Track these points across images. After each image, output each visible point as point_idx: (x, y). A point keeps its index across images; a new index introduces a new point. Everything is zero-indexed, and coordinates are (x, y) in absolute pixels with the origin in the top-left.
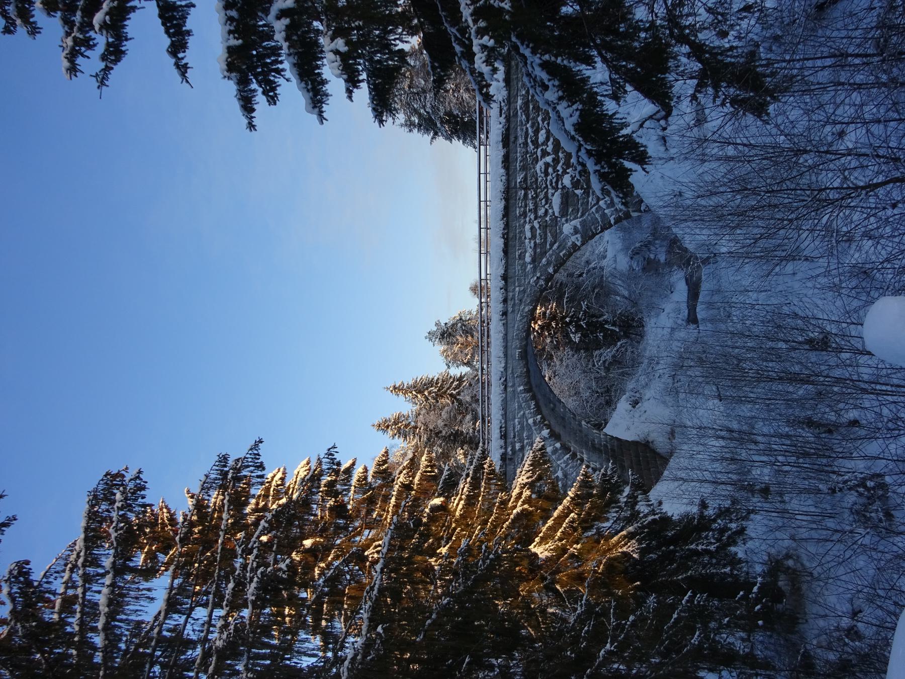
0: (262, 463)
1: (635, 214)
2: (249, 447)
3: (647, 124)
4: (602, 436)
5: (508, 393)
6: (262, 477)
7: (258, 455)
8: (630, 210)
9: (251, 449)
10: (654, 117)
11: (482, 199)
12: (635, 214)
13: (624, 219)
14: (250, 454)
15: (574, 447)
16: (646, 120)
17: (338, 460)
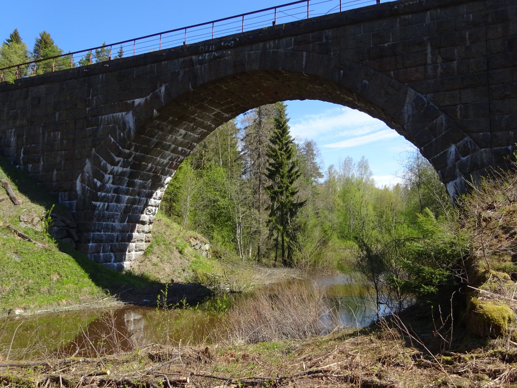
5: (190, 58)
8: (458, 180)
15: (130, 155)
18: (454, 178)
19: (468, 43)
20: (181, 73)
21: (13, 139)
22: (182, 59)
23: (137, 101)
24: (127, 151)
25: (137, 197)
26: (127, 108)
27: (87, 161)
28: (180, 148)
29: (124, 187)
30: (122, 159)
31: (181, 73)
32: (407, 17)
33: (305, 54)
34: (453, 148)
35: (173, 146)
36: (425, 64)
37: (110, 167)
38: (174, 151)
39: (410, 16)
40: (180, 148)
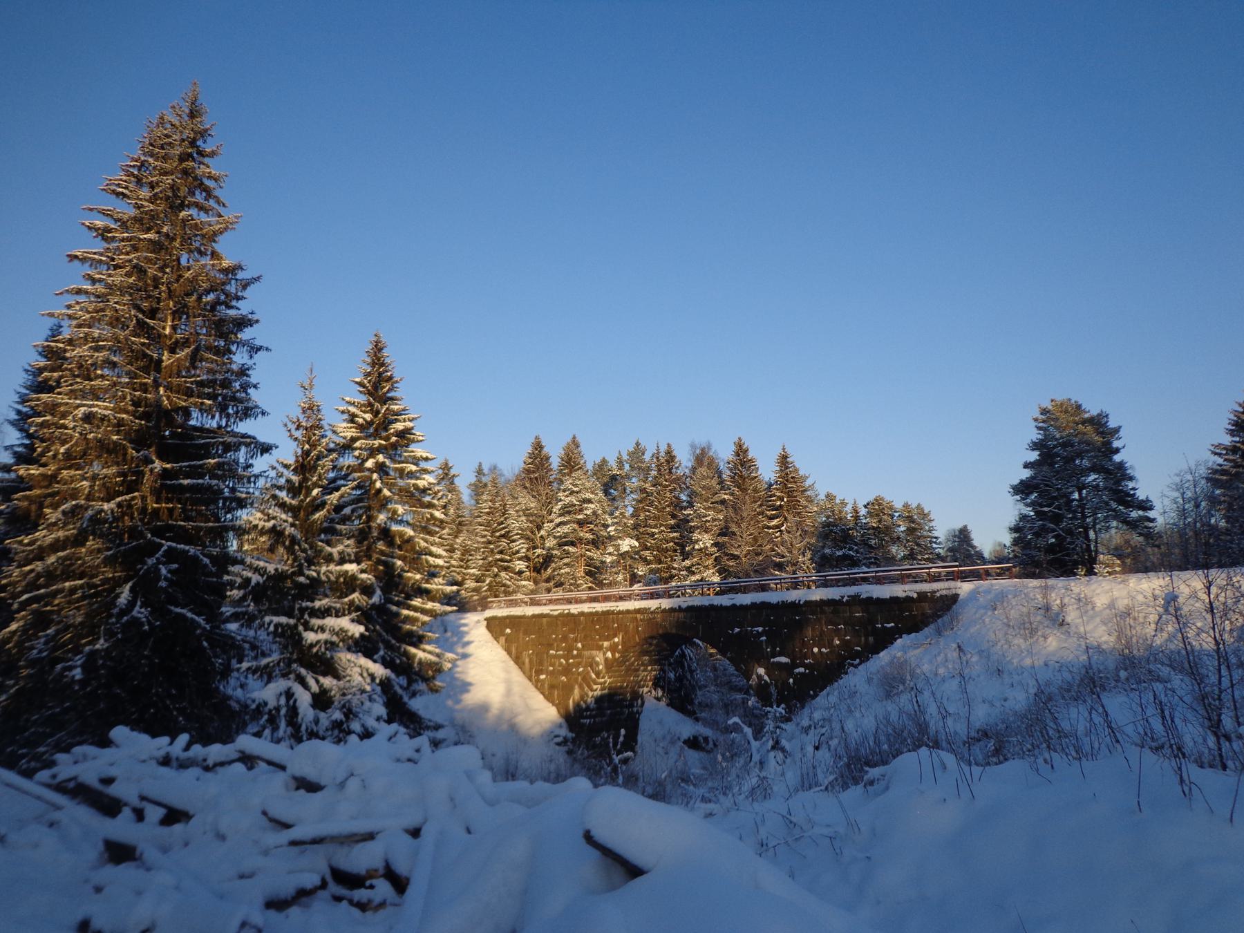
4: (635, 709)
15: (605, 682)
20: (631, 626)
21: (527, 661)
22: (631, 615)
23: (606, 644)
24: (603, 680)
25: (619, 709)
26: (600, 648)
27: (576, 687)
28: (649, 668)
29: (606, 704)
30: (599, 686)
31: (631, 626)
35: (642, 668)
37: (590, 694)
38: (644, 671)
39: (754, 611)
40: (649, 668)
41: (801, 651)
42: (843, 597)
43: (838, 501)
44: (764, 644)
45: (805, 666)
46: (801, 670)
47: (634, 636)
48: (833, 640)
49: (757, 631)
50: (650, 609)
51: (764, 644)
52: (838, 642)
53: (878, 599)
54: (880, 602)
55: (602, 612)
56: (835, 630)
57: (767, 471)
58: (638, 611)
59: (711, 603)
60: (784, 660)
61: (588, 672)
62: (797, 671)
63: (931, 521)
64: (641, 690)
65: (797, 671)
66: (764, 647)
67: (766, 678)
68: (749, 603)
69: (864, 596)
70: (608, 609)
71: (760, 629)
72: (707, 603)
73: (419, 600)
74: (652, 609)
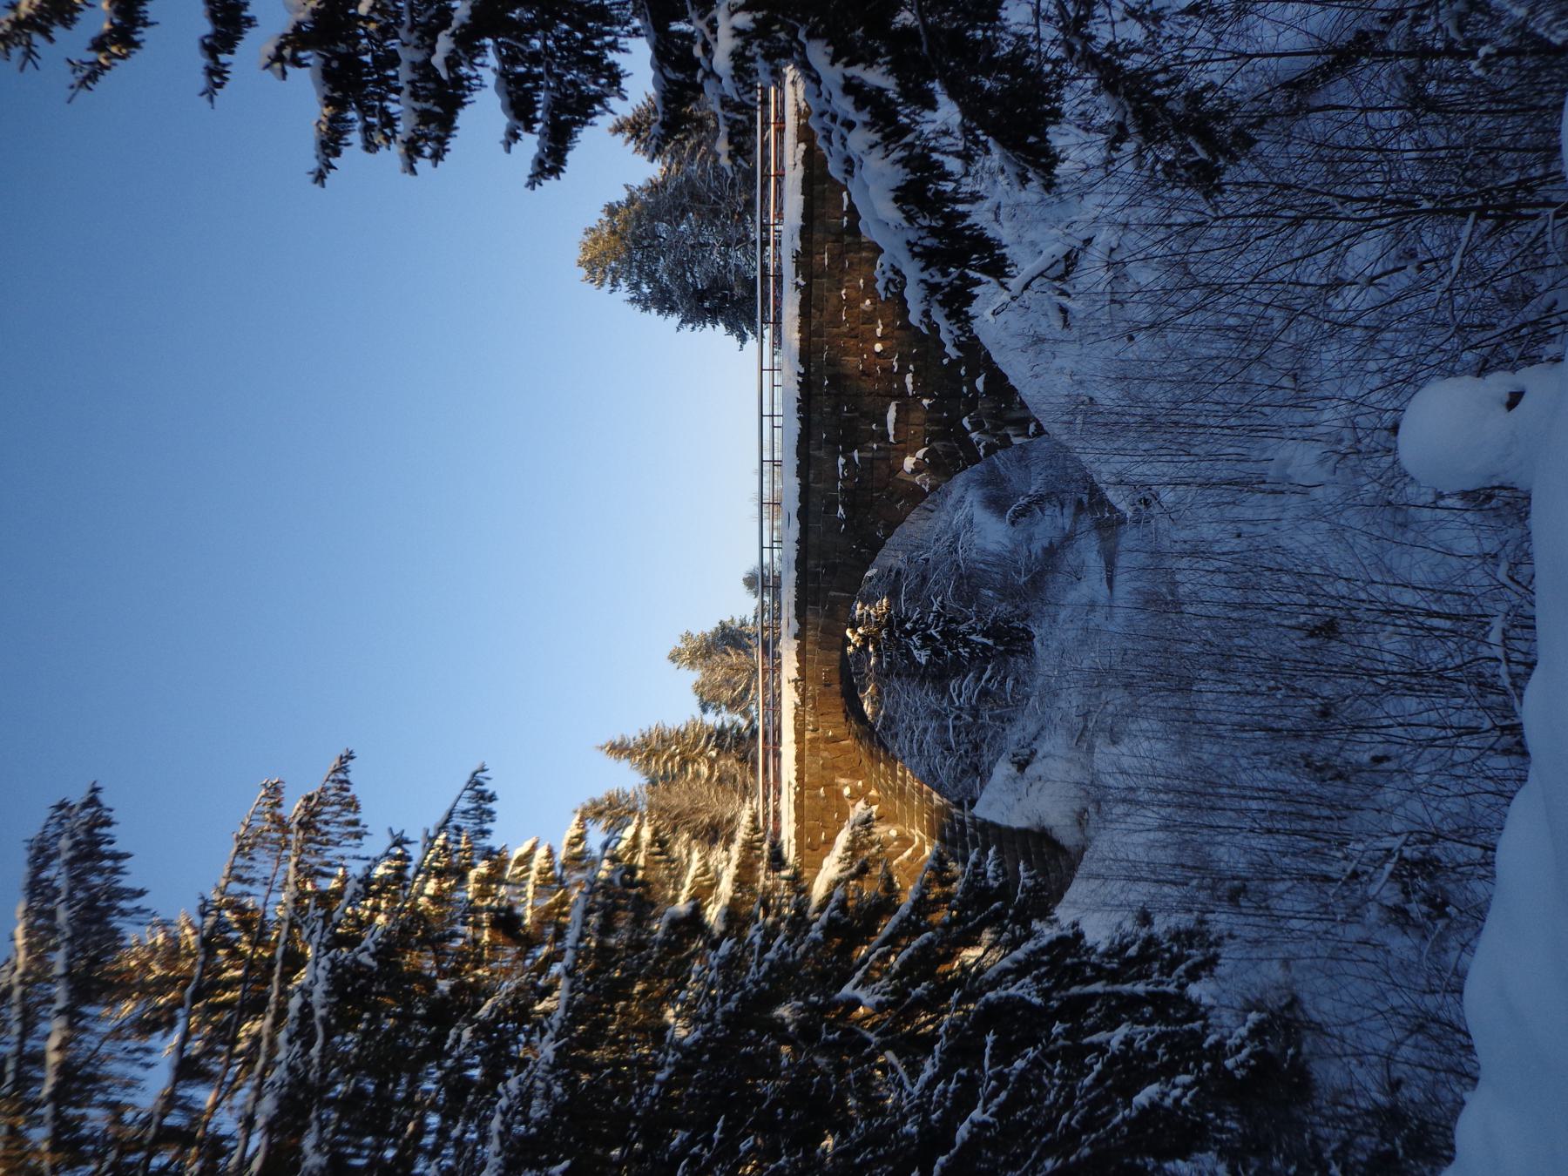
0: (353, 797)
1: (1017, 441)
2: (332, 769)
3: (1034, 284)
4: (967, 819)
6: (355, 823)
7: (347, 782)
8: (1011, 433)
9: (335, 771)
10: (1049, 273)
11: (766, 411)
12: (1017, 441)
13: (1001, 448)
14: (333, 781)
16: (1033, 279)
17: (490, 792)
18: (1008, 435)
19: (857, 414)
20: (825, 754)
22: (807, 753)
31: (825, 754)
32: (811, 476)
33: (832, 593)
34: (974, 435)
36: (873, 459)
41: (879, 379)
42: (798, 286)
43: (683, 646)
44: (863, 454)
45: (903, 370)
46: (909, 379)
47: (845, 751)
48: (865, 312)
49: (844, 466)
50: (797, 707)
51: (863, 454)
52: (868, 302)
53: (804, 217)
54: (808, 215)
55: (797, 821)
56: (849, 307)
57: (628, 779)
58: (799, 740)
59: (793, 565)
60: (891, 415)
61: (900, 864)
62: (910, 387)
63: (732, 621)
64: (935, 802)
65: (910, 387)
66: (869, 455)
67: (920, 454)
68: (798, 480)
69: (798, 244)
70: (792, 806)
71: (841, 461)
72: (794, 574)
73: (709, 910)
74: (798, 700)
